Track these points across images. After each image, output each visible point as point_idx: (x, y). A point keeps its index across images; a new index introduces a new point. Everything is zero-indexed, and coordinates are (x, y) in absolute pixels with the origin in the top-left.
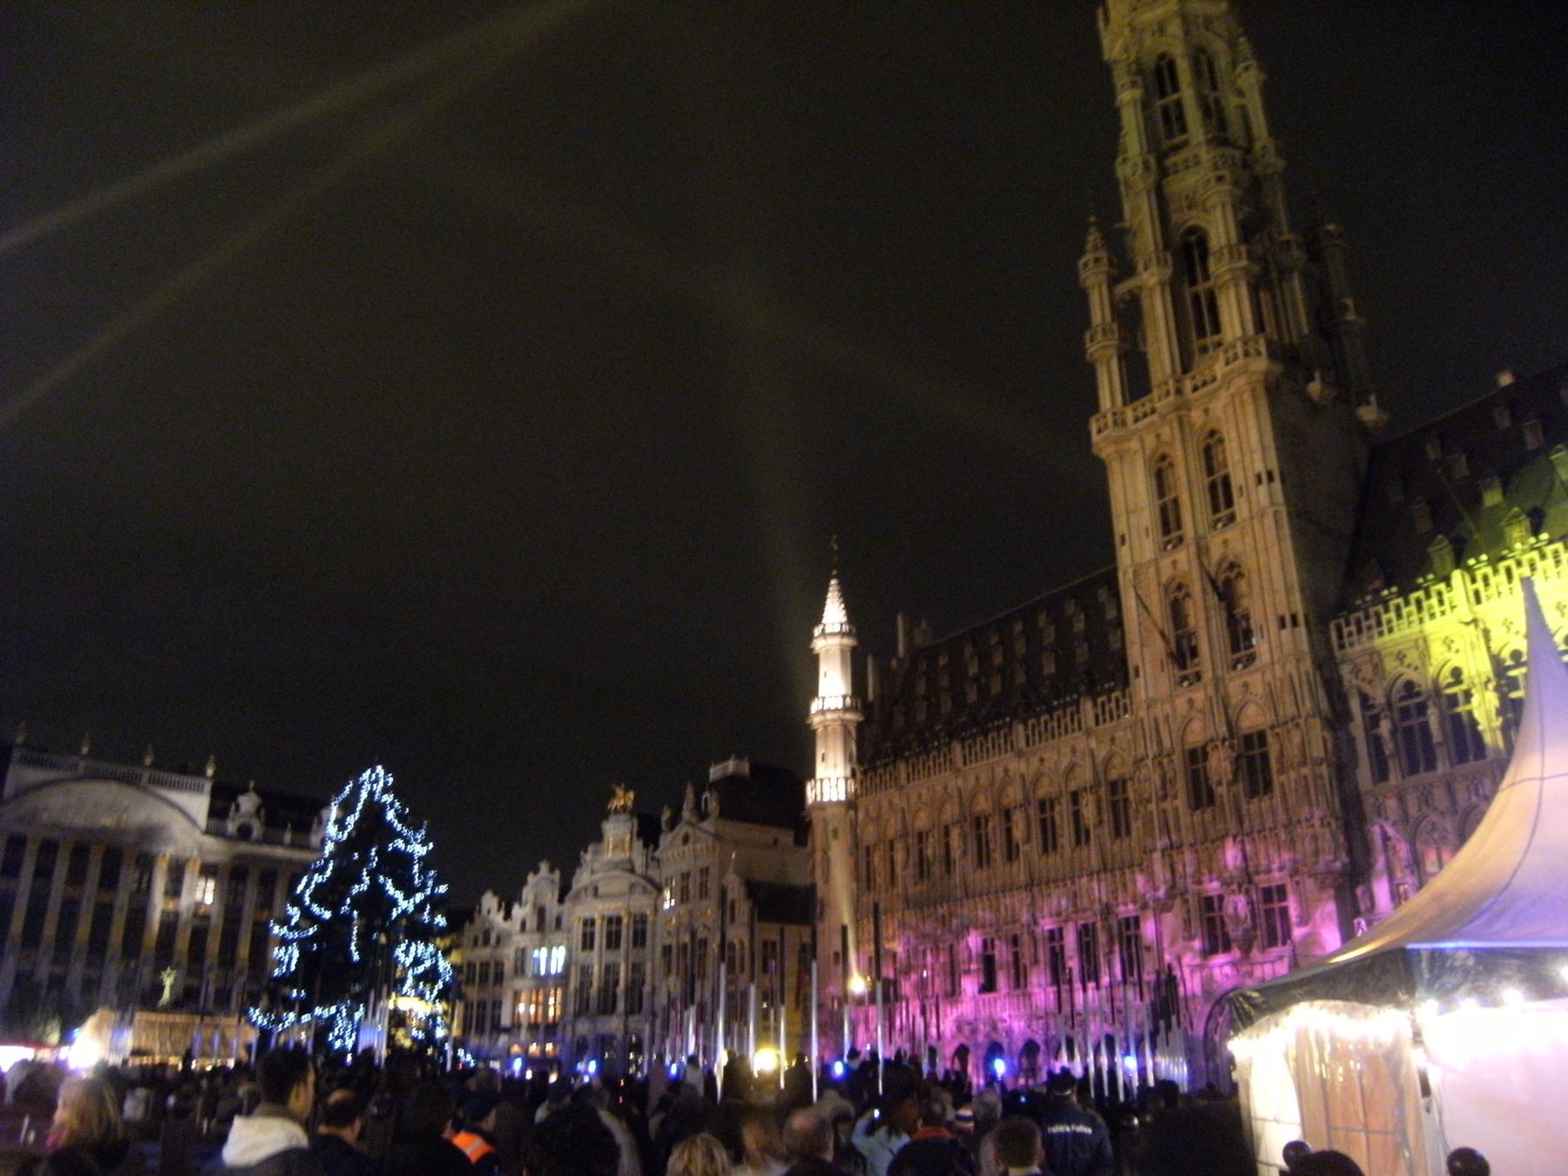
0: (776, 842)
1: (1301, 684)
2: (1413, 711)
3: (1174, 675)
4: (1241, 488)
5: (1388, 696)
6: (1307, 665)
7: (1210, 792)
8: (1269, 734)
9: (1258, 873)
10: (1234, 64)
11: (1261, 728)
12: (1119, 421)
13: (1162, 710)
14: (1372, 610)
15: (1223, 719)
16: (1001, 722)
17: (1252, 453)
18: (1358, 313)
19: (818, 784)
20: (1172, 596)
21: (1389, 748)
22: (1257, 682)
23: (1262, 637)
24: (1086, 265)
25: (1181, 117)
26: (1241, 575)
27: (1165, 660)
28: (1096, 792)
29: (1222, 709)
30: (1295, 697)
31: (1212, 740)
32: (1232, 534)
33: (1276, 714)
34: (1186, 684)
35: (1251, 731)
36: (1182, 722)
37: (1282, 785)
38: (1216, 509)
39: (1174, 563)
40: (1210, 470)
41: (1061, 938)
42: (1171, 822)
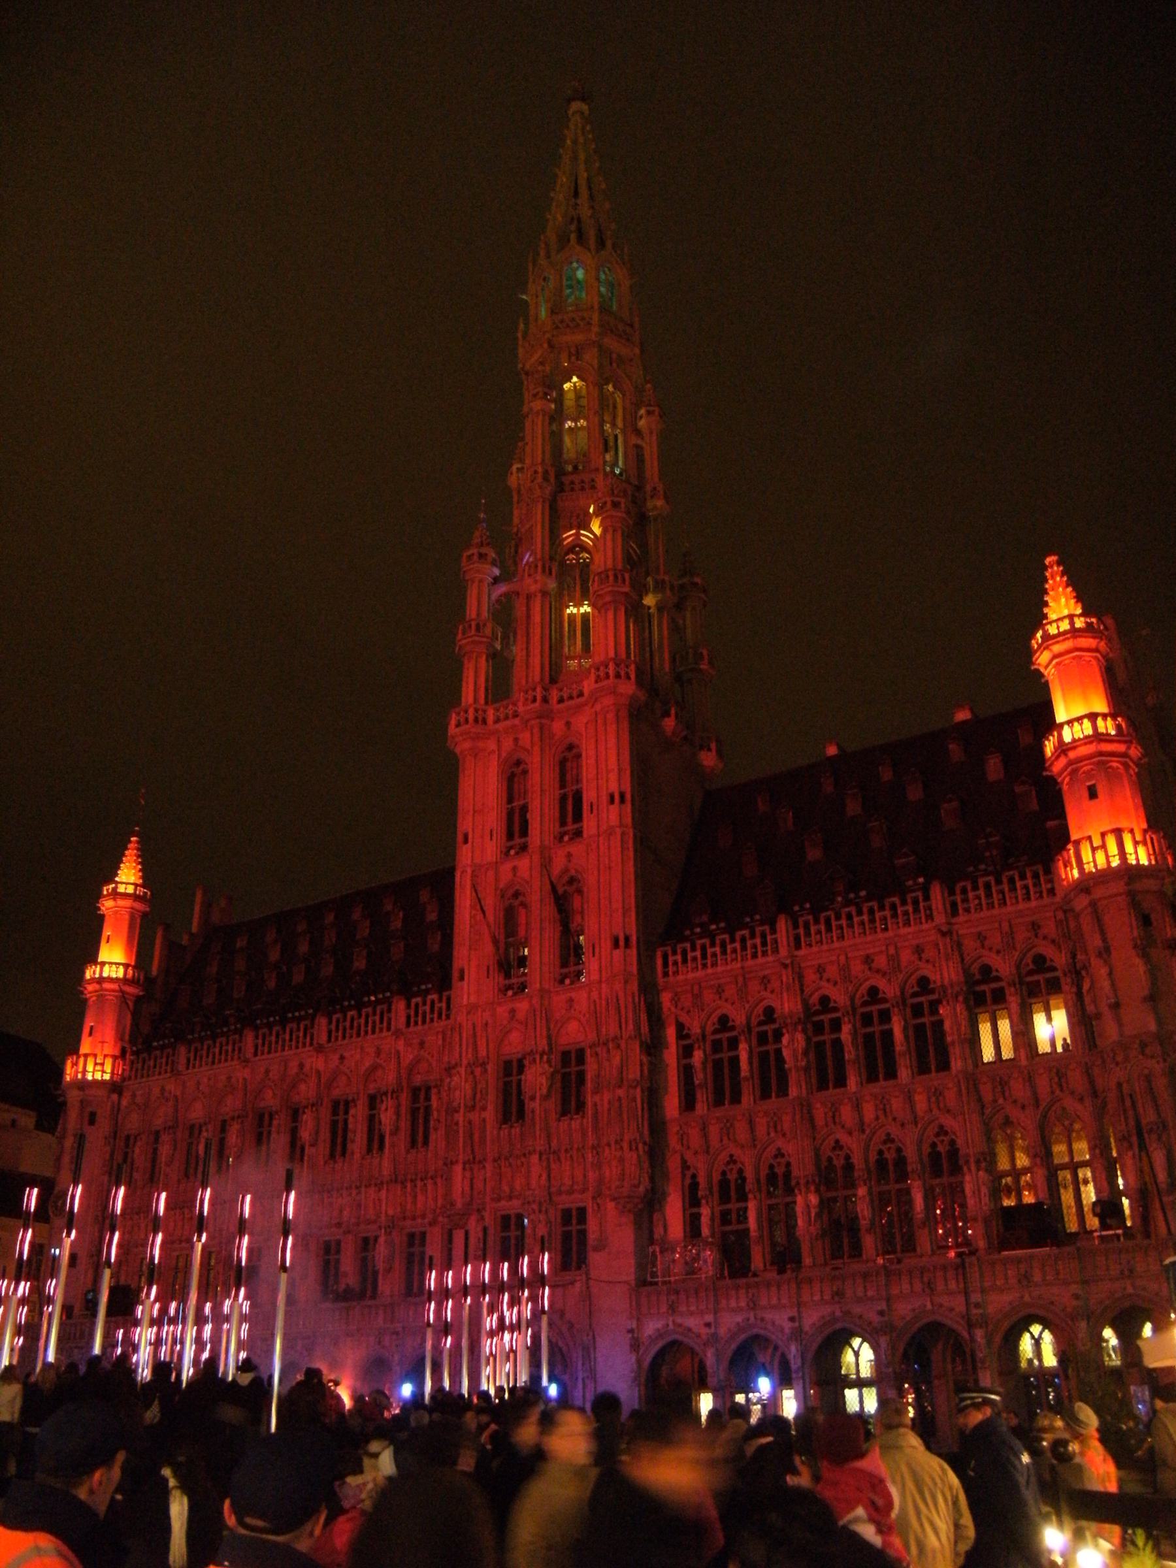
1: (626, 1007)
5: (703, 1028)
6: (634, 986)
7: (521, 1104)
8: (588, 1052)
9: (560, 1193)
12: (480, 719)
14: (699, 942)
15: (545, 1033)
16: (303, 1013)
17: (608, 771)
19: (82, 1060)
21: (698, 1078)
22: (581, 997)
26: (579, 891)
28: (397, 1098)
29: (544, 1021)
32: (576, 849)
34: (510, 993)
35: (567, 1048)
37: (595, 1105)
38: (563, 823)
41: (338, 1252)
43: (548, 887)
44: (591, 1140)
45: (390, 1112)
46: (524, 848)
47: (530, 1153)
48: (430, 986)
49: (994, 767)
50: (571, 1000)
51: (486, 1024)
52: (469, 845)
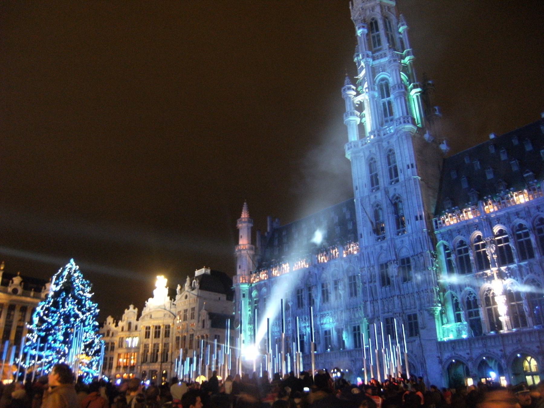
1: (423, 240)
3: (375, 237)
5: (453, 246)
9: (406, 309)
10: (398, 23)
11: (407, 257)
13: (371, 250)
15: (394, 253)
17: (405, 157)
18: (440, 112)
20: (374, 209)
23: (409, 224)
24: (344, 90)
25: (379, 41)
26: (401, 202)
27: (372, 232)
28: (344, 280)
29: (393, 249)
30: (422, 246)
32: (398, 186)
33: (414, 251)
34: (379, 240)
35: (403, 258)
36: (378, 254)
38: (391, 178)
39: (376, 197)
40: (389, 164)
42: (374, 291)
43: (389, 201)
46: (378, 189)
47: (394, 296)
48: (350, 241)
50: (402, 241)
51: (372, 252)
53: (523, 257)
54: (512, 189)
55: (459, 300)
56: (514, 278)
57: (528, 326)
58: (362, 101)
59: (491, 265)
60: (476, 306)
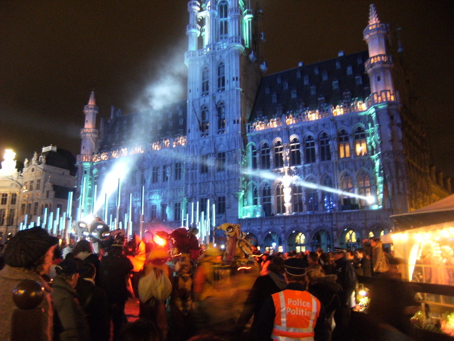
0: (64, 173)
1: (237, 140)
2: (325, 142)
3: (200, 134)
4: (228, 81)
5: (260, 147)
8: (226, 154)
9: (218, 193)
11: (223, 152)
13: (196, 143)
17: (233, 71)
18: (264, 37)
20: (203, 110)
22: (224, 138)
23: (228, 125)
26: (224, 107)
28: (171, 166)
29: (213, 145)
30: (235, 144)
31: (210, 154)
32: (223, 94)
33: (229, 148)
34: (203, 136)
38: (219, 86)
39: (205, 100)
40: (219, 74)
42: (194, 177)
43: (214, 106)
44: (227, 178)
45: (170, 170)
46: (207, 94)
47: (209, 182)
48: (180, 134)
49: (349, 70)
52: (191, 93)
53: (307, 162)
54: (308, 108)
55: (258, 189)
56: (299, 176)
57: (303, 211)
58: (204, 17)
59: (284, 165)
60: (270, 194)
